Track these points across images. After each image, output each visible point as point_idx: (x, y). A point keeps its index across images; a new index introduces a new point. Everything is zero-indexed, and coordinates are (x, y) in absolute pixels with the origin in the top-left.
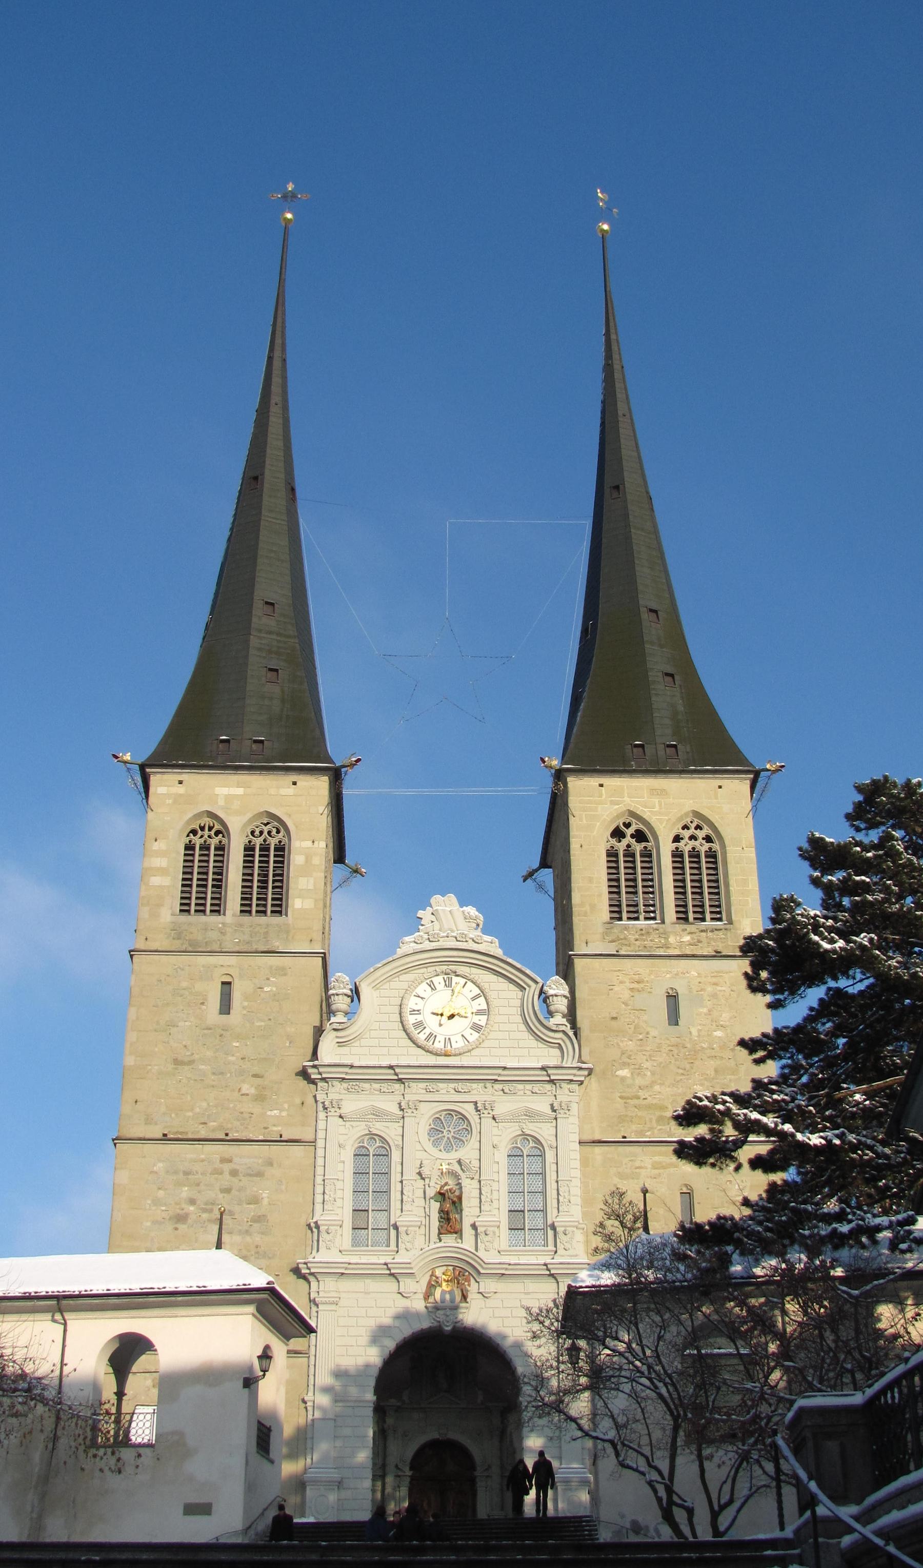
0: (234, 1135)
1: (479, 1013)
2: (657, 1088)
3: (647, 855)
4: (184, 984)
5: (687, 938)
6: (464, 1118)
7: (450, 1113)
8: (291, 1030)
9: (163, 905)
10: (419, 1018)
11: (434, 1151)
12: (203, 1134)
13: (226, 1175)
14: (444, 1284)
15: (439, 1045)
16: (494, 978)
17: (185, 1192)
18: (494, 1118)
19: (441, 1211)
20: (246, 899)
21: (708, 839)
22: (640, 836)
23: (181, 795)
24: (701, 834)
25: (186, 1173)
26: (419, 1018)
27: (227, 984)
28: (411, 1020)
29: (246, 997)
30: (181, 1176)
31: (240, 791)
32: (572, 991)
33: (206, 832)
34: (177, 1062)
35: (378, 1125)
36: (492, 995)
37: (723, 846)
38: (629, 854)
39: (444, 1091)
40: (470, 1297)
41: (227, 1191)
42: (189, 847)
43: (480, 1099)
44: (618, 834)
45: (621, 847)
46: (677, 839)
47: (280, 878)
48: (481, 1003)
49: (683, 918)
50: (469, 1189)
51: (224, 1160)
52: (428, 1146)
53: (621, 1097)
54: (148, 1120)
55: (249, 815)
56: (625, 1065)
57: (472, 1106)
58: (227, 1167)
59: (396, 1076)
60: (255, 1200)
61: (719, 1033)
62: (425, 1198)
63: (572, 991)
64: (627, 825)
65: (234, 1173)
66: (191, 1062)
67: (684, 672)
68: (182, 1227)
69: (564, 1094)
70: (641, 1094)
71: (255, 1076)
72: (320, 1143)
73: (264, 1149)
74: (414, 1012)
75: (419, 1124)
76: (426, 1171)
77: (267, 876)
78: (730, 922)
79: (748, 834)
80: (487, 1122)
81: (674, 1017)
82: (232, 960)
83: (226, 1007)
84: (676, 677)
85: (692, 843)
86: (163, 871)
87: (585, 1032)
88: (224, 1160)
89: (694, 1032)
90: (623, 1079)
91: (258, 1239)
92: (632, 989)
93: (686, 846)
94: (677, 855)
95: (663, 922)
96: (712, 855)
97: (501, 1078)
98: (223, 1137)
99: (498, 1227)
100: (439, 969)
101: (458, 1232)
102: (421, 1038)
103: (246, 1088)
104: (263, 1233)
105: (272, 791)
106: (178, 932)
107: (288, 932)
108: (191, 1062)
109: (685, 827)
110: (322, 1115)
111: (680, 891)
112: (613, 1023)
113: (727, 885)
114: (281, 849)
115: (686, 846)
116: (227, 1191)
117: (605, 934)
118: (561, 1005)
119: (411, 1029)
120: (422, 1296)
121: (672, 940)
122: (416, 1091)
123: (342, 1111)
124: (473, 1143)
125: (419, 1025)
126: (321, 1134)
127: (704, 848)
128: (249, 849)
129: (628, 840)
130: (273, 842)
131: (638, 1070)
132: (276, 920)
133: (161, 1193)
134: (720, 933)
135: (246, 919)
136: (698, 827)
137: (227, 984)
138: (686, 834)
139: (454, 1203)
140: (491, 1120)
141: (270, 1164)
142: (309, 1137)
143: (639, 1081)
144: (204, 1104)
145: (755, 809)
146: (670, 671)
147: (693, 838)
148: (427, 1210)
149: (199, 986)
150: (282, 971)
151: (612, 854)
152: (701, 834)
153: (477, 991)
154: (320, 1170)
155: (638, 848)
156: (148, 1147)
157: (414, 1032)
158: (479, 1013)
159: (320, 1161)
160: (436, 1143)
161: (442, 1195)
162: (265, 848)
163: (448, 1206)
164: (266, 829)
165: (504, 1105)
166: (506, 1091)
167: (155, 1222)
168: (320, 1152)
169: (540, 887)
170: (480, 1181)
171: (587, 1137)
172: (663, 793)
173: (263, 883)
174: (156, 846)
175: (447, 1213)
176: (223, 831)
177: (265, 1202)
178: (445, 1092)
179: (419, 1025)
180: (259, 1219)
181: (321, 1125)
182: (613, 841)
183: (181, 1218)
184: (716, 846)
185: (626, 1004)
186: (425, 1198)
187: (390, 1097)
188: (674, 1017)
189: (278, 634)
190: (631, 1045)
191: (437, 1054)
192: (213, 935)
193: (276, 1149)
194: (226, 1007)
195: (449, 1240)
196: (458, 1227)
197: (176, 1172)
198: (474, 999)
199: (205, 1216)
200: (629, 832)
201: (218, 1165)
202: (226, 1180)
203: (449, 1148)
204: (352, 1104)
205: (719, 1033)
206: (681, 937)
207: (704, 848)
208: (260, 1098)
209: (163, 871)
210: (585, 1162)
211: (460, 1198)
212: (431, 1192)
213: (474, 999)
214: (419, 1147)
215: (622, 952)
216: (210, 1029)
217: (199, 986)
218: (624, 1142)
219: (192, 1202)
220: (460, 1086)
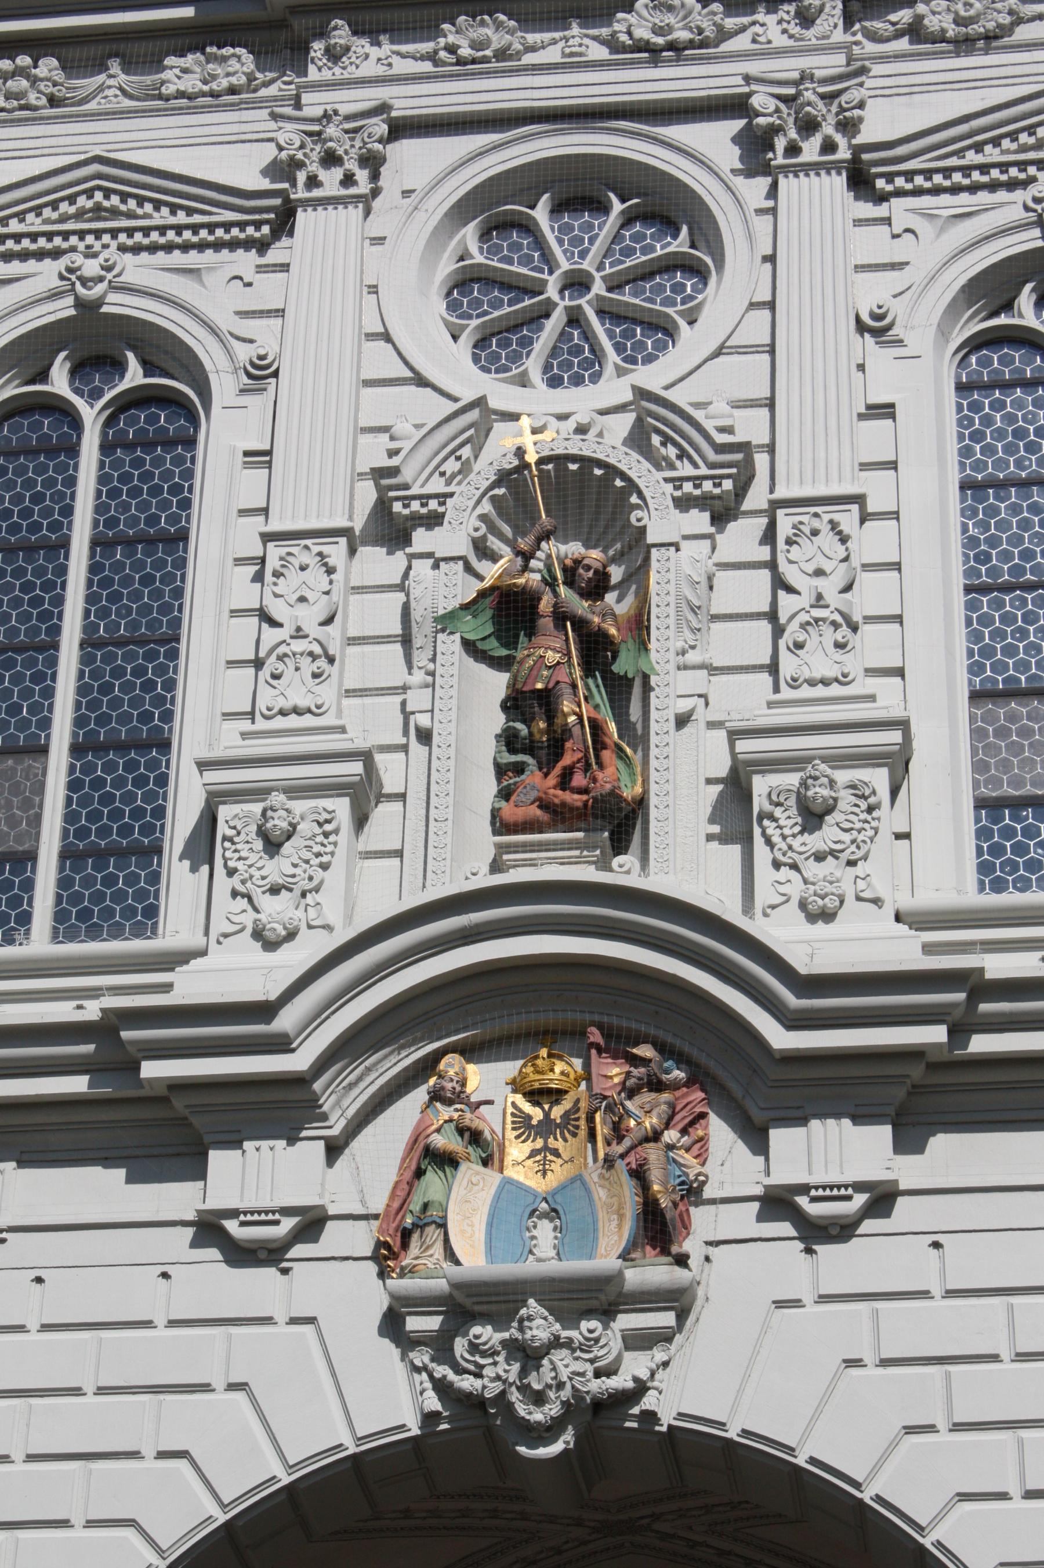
6: (663, 205)
7: (580, 190)
14: (517, 1151)
18: (860, 181)
19: (515, 704)
35: (136, 269)
39: (552, 55)
40: (704, 1224)
50: (683, 554)
57: (717, 140)
62: (406, 640)
76: (419, 478)
99: (898, 764)
101: (620, 822)
120: (361, 1239)
139: (596, 650)
140: (840, 181)
148: (417, 700)
160: (498, 345)
161: (510, 614)
163: (551, 653)
166: (932, 23)
170: (769, 536)
175: (547, 700)
186: (406, 640)
187: (226, 122)
196: (613, 776)
203: (575, 364)
211: (639, 625)
214: (382, 361)
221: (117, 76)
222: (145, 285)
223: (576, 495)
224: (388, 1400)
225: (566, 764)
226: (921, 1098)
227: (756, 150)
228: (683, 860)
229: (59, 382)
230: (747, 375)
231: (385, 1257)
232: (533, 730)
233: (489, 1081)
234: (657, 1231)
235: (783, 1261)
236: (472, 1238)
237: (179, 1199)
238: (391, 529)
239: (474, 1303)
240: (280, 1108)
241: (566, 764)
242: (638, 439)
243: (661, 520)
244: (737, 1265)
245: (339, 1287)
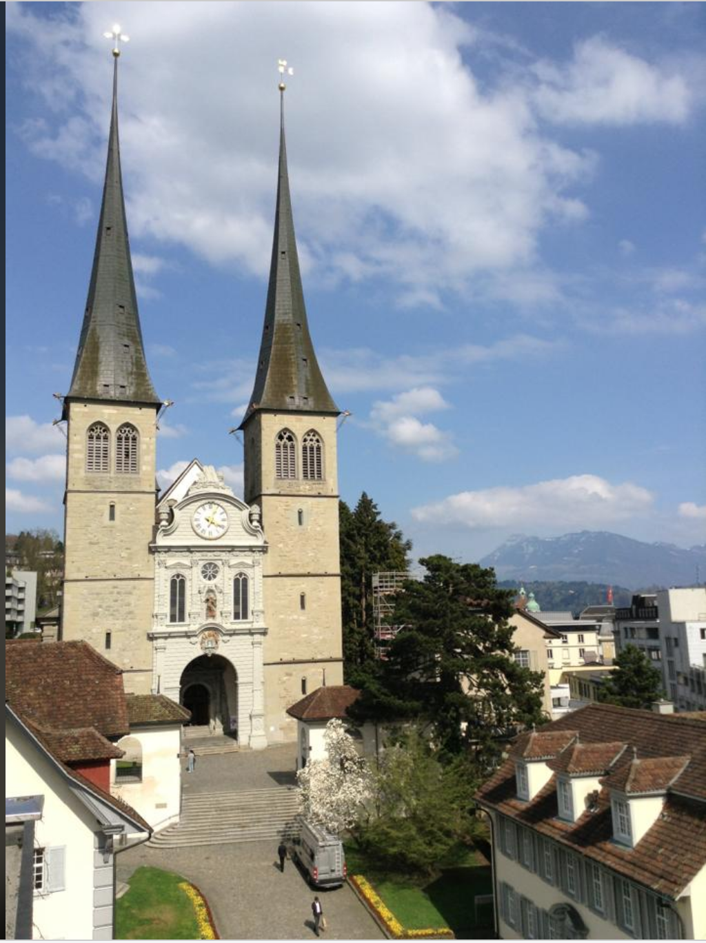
0: (119, 576)
1: (224, 520)
2: (294, 552)
3: (293, 447)
4: (93, 507)
5: (307, 487)
7: (210, 564)
8: (142, 527)
9: (79, 468)
10: (198, 522)
11: (204, 580)
12: (104, 577)
13: (115, 595)
15: (206, 535)
16: (229, 505)
17: (97, 603)
18: (229, 567)
20: (119, 463)
21: (318, 441)
22: (290, 439)
23: (86, 413)
24: (315, 439)
25: (98, 594)
26: (198, 522)
27: (112, 507)
28: (195, 523)
29: (122, 513)
30: (95, 596)
31: (115, 412)
32: (261, 511)
33: (99, 430)
34: (91, 543)
36: (229, 512)
37: (324, 446)
38: (285, 447)
41: (116, 601)
42: (91, 437)
43: (224, 558)
44: (281, 438)
45: (282, 443)
46: (305, 440)
47: (134, 453)
48: (224, 516)
49: (305, 476)
50: (219, 597)
51: (115, 587)
52: (202, 577)
53: (280, 556)
54: (79, 570)
55: (119, 424)
56: (281, 542)
58: (116, 590)
59: (189, 549)
60: (129, 605)
61: (318, 529)
63: (261, 511)
64: (285, 434)
65: (118, 593)
66: (97, 543)
67: (310, 358)
68: (97, 618)
69: (257, 556)
70: (288, 554)
71: (127, 549)
72: (156, 579)
73: (132, 582)
74: (196, 520)
75: (197, 570)
77: (128, 452)
78: (325, 480)
79: (335, 440)
80: (226, 568)
81: (300, 522)
82: (115, 495)
83: (112, 517)
84: (308, 361)
85: (311, 443)
86: (79, 451)
87: (265, 528)
88: (115, 587)
89: (309, 527)
90: (281, 548)
91: (130, 621)
92: (285, 510)
93: (308, 444)
94: (305, 449)
95: (298, 479)
96: (319, 448)
97: (232, 549)
98: (113, 577)
100: (207, 501)
101: (213, 617)
102: (199, 531)
103: (123, 554)
104: (131, 619)
105: (131, 412)
106: (88, 481)
107: (140, 482)
108: (97, 543)
109: (309, 435)
110: (157, 566)
111: (305, 464)
112: (277, 525)
113: (324, 462)
114: (134, 439)
115: (308, 444)
116: (116, 601)
117: (276, 484)
118: (256, 517)
119: (201, 534)
121: (301, 488)
122: (197, 556)
123: (167, 565)
124: (219, 576)
125: (198, 526)
126: (156, 575)
127: (315, 445)
128: (119, 439)
129: (285, 440)
130: (131, 436)
131: (286, 545)
132: (134, 476)
133: (86, 604)
134: (321, 486)
135: (119, 475)
136: (314, 436)
137: (112, 507)
138: (309, 438)
139: (212, 603)
141: (134, 588)
142: (152, 577)
143: (287, 549)
144: (104, 562)
145: (338, 429)
146: (305, 358)
147: (311, 440)
149: (100, 507)
150: (138, 500)
151: (278, 447)
152: (315, 439)
153: (222, 510)
154: (156, 591)
155: (289, 444)
156: (79, 583)
157: (196, 529)
158: (224, 520)
159: (156, 587)
160: (205, 577)
161: (207, 600)
162: (127, 439)
163: (210, 604)
164: (127, 429)
165: (234, 561)
167: (85, 617)
168: (156, 583)
169: (238, 438)
171: (265, 574)
172: (301, 420)
173: (127, 456)
174: (75, 438)
176: (106, 429)
177: (133, 605)
178: (210, 556)
179: (198, 526)
180: (130, 613)
181: (157, 571)
182: (279, 441)
183: (95, 614)
184: (321, 444)
185: (282, 516)
188: (300, 522)
189: (128, 325)
190: (283, 533)
191: (206, 539)
192: (105, 483)
193: (137, 582)
194: (112, 517)
195: (211, 620)
197: (92, 594)
198: (221, 514)
199: (107, 612)
200: (285, 436)
201: (111, 590)
202: (115, 596)
203: (210, 579)
204: (171, 560)
205: (318, 529)
206: (305, 487)
207: (315, 445)
208: (130, 559)
209: (79, 451)
210: (264, 584)
211: (216, 600)
212: (204, 599)
213: (221, 514)
215: (282, 493)
216: (105, 527)
217: (100, 507)
218: (280, 575)
219: (100, 607)
220: (215, 553)
221: (179, 554)
222: (182, 571)
223: (210, 591)
224: (201, 653)
225: (210, 611)
226: (231, 635)
227: (223, 564)
228: (218, 620)
229: (175, 578)
230: (221, 582)
231: (201, 644)
232: (209, 609)
233: (206, 633)
234: (217, 642)
235: (223, 644)
236: (205, 645)
237: (189, 640)
238: (200, 592)
239: (206, 648)
240: (195, 636)
241: (210, 611)
242: (216, 586)
243: (217, 594)
244: (220, 643)
245: (198, 646)
